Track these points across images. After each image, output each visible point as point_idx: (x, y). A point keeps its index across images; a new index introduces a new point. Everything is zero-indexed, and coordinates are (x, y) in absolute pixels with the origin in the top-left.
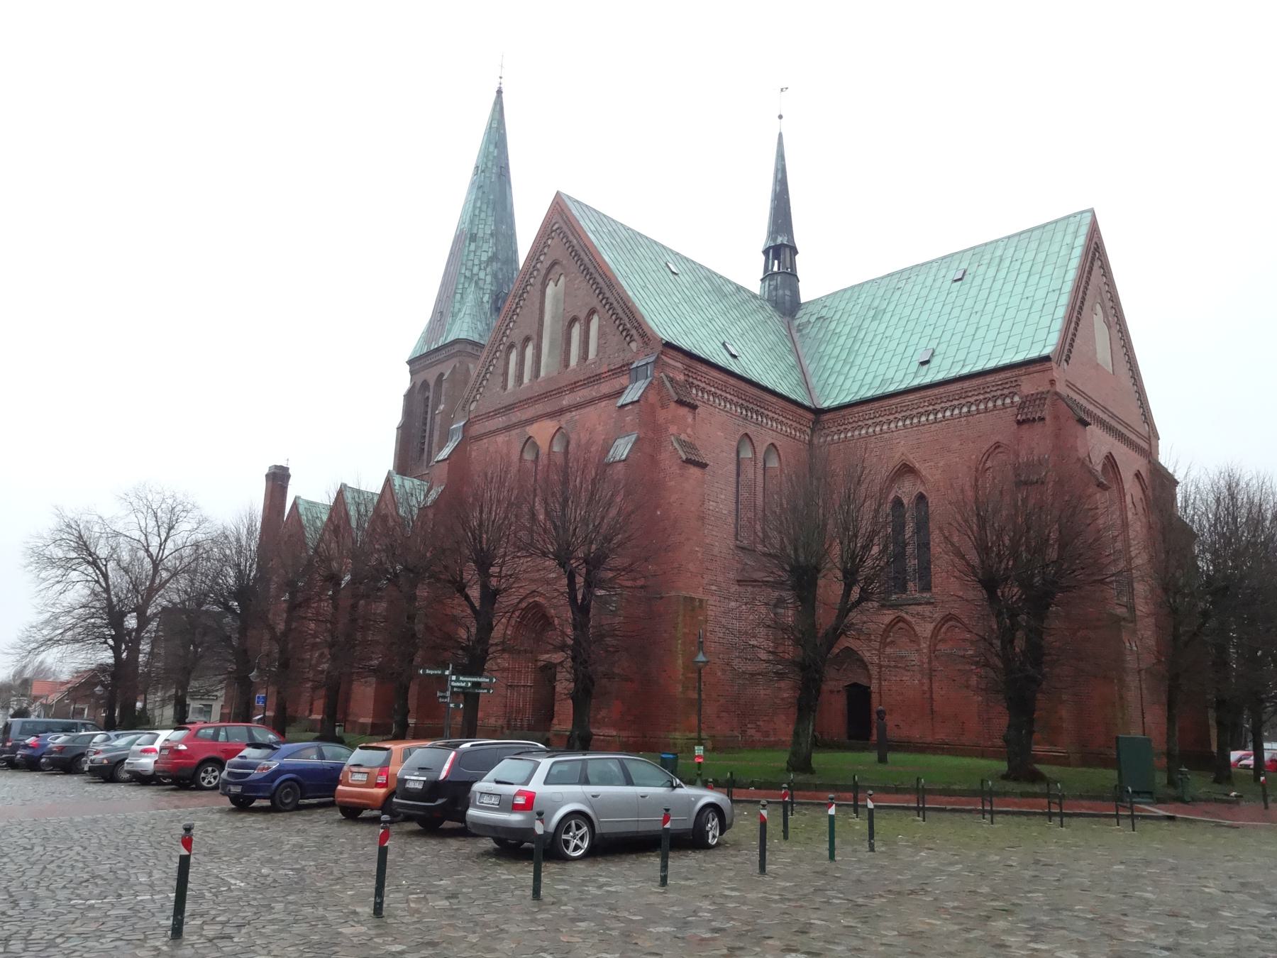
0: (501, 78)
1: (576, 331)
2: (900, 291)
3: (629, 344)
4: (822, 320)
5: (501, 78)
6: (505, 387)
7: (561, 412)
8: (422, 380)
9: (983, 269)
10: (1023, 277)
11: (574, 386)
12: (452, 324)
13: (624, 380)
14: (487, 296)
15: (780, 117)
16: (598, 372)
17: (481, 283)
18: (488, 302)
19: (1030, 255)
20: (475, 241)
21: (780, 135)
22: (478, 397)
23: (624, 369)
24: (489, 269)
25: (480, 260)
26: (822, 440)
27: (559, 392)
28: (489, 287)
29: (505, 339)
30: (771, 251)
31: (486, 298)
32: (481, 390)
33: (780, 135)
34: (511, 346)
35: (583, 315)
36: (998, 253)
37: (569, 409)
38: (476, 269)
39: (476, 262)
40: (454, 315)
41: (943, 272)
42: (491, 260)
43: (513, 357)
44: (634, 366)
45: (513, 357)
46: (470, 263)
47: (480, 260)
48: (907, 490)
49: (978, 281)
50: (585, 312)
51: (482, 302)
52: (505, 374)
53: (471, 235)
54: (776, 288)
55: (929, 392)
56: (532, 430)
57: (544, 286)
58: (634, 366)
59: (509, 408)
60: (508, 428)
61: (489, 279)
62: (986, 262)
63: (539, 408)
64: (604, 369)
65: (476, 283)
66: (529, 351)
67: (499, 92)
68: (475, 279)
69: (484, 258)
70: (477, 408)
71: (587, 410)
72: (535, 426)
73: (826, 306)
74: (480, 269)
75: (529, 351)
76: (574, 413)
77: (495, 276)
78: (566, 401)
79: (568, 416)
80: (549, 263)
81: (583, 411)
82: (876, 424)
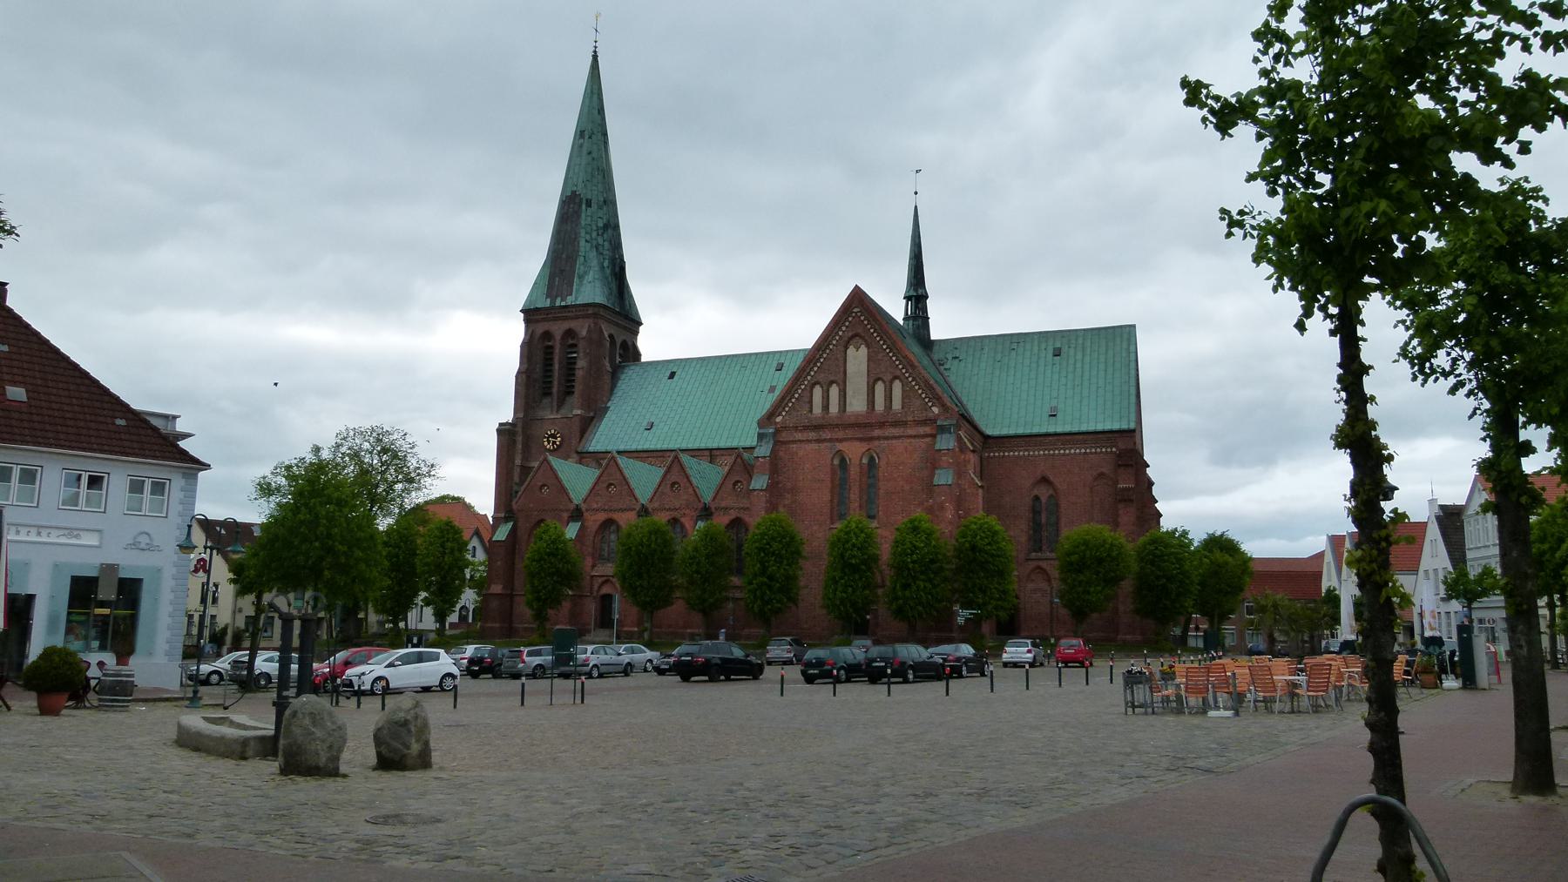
0: (596, 42)
1: (880, 388)
2: (1014, 353)
3: (930, 407)
4: (957, 360)
5: (596, 42)
6: (811, 411)
7: (871, 439)
8: (541, 331)
9: (1072, 352)
10: (1102, 366)
11: (882, 425)
12: (581, 284)
13: (927, 430)
14: (607, 261)
15: (916, 193)
16: (904, 419)
17: (601, 249)
18: (608, 267)
19: (1103, 350)
20: (591, 207)
21: (916, 207)
22: (784, 413)
23: (924, 422)
24: (605, 235)
25: (597, 226)
26: (986, 455)
27: (870, 426)
28: (607, 252)
29: (809, 378)
30: (913, 298)
31: (606, 264)
32: (787, 409)
33: (916, 207)
34: (815, 383)
35: (888, 377)
36: (1080, 341)
37: (878, 438)
38: (594, 234)
39: (595, 228)
40: (581, 277)
41: (1043, 346)
42: (606, 227)
43: (818, 392)
44: (939, 423)
45: (818, 392)
46: (589, 229)
47: (597, 226)
48: (1044, 493)
49: (1071, 361)
50: (890, 377)
51: (604, 267)
52: (811, 402)
53: (587, 200)
54: (918, 327)
55: (1062, 437)
56: (839, 446)
57: (846, 348)
58: (939, 423)
59: (817, 427)
60: (819, 441)
61: (606, 244)
62: (1073, 346)
63: (850, 433)
64: (910, 418)
65: (597, 249)
66: (834, 391)
67: (595, 57)
68: (594, 243)
69: (601, 225)
70: (784, 421)
71: (894, 441)
72: (845, 444)
73: (956, 348)
74: (598, 235)
75: (834, 391)
76: (882, 442)
77: (611, 244)
78: (877, 433)
79: (876, 443)
80: (850, 334)
81: (890, 442)
82: (1027, 450)
